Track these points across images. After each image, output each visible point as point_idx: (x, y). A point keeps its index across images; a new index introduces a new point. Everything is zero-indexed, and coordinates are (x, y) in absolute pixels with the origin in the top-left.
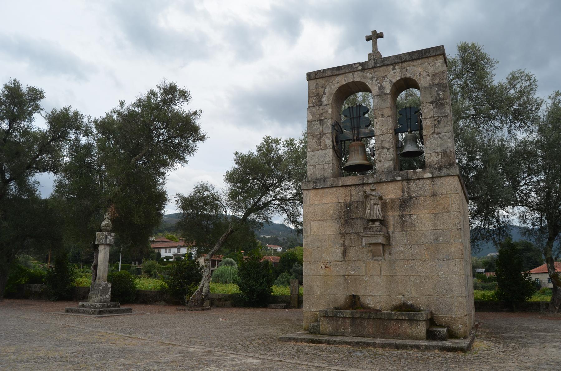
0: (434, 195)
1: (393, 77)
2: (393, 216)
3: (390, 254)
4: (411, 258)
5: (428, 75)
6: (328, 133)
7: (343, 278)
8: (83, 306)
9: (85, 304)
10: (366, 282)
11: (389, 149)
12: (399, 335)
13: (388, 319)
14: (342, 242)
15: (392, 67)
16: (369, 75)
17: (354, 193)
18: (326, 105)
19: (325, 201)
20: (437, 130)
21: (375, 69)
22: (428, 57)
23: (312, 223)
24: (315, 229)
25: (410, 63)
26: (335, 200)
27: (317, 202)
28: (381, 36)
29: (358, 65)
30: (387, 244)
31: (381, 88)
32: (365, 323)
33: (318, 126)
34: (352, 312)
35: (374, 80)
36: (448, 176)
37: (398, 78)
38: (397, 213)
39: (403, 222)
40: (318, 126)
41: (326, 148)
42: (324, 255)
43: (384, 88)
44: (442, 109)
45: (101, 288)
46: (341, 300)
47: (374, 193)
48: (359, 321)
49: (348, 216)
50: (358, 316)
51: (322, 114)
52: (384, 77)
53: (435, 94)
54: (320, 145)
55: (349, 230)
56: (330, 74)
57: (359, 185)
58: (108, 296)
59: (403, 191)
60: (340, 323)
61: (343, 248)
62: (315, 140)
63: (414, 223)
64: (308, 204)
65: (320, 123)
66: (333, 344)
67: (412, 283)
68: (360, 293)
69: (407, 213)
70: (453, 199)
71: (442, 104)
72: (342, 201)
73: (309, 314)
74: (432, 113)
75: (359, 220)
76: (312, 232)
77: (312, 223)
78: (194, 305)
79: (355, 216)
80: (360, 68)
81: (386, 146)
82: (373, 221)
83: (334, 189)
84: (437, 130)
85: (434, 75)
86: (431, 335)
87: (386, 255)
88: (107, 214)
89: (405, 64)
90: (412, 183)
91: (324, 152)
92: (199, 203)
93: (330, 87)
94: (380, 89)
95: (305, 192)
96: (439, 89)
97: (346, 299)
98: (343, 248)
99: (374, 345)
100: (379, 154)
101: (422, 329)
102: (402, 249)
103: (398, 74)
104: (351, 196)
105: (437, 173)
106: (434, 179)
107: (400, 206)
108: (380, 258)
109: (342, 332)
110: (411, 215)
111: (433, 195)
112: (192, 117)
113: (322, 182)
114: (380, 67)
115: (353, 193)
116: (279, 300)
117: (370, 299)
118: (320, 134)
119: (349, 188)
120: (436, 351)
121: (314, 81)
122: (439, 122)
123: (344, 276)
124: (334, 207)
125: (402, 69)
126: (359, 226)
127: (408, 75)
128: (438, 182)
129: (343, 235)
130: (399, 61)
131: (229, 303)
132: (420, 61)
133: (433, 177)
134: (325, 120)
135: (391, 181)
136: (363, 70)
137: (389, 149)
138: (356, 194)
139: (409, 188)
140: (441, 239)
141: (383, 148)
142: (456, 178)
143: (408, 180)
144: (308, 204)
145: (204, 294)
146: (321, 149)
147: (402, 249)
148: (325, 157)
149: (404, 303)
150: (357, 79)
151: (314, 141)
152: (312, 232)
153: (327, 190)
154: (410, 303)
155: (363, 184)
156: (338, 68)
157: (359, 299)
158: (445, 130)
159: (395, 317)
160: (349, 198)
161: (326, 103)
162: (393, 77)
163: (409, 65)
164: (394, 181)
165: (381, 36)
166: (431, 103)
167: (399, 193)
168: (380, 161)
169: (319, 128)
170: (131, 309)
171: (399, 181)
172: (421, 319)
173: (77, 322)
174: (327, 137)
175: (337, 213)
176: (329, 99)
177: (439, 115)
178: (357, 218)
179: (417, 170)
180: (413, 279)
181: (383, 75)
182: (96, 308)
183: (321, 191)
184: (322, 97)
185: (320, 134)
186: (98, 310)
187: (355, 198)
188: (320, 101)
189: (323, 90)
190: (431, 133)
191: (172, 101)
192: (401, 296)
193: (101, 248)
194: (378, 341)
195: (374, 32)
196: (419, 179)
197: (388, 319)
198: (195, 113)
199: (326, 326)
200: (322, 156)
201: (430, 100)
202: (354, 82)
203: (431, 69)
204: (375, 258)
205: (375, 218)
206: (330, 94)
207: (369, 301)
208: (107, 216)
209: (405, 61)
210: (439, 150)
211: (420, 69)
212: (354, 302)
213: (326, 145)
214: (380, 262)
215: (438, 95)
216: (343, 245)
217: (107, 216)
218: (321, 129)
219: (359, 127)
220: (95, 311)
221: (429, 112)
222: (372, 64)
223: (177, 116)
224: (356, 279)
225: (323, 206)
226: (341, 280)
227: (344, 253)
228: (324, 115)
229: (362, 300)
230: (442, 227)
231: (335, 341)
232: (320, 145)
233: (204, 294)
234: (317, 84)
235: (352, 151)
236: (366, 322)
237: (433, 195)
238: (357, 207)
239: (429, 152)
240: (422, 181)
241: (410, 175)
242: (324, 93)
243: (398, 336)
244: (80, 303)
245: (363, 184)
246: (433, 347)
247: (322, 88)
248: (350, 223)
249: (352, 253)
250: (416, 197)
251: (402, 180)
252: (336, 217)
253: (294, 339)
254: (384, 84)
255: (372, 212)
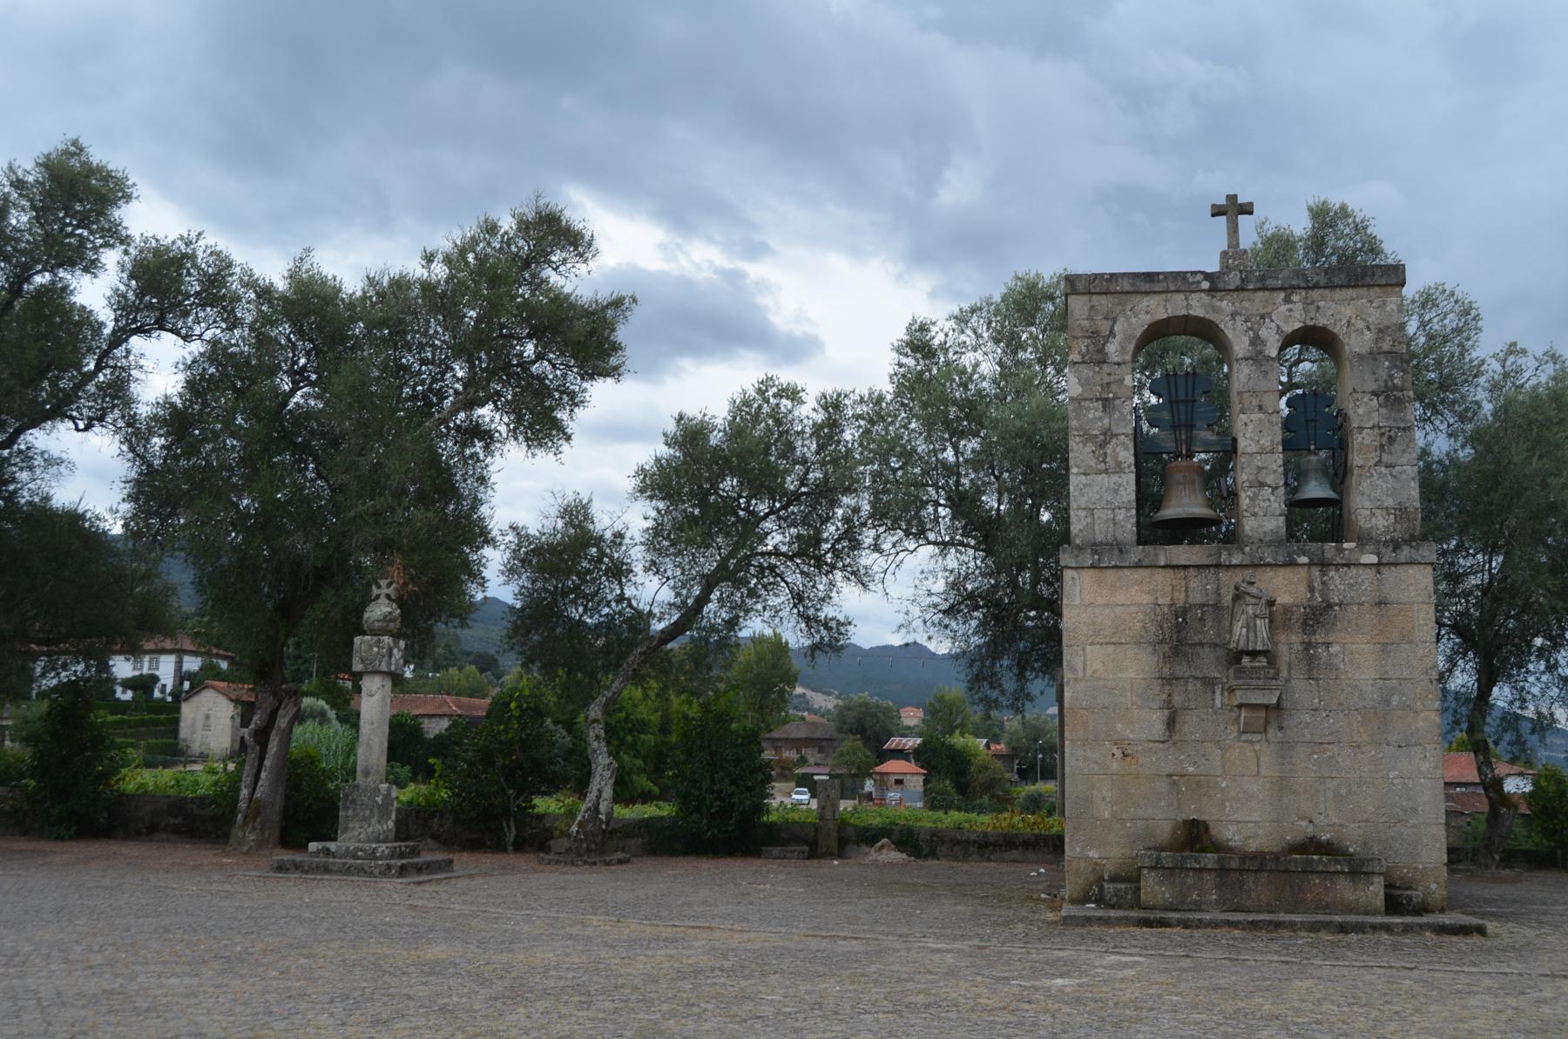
0: (1381, 603)
1: (1287, 319)
2: (1289, 644)
3: (1281, 728)
4: (1329, 739)
5: (1368, 328)
6: (1127, 435)
7: (1167, 780)
8: (327, 852)
9: (332, 846)
10: (1222, 790)
11: (1275, 489)
12: (1327, 907)
13: (1304, 872)
14: (1164, 697)
15: (1282, 295)
16: (1226, 305)
17: (1194, 584)
18: (1118, 364)
19: (1121, 598)
20: (1386, 458)
21: (1245, 294)
22: (1368, 286)
23: (1089, 648)
24: (1097, 665)
25: (1327, 292)
26: (1147, 599)
27: (1100, 601)
28: (1247, 209)
29: (1199, 277)
30: (1275, 712)
31: (1256, 341)
32: (1250, 881)
33: (1099, 414)
34: (1220, 859)
35: (1239, 319)
36: (1412, 563)
37: (1298, 325)
38: (1296, 639)
39: (1310, 659)
40: (1099, 414)
41: (1119, 469)
42: (1119, 726)
43: (1263, 343)
44: (1400, 411)
45: (379, 799)
46: (1164, 830)
47: (1253, 590)
48: (1235, 876)
49: (1178, 637)
50: (1234, 865)
51: (1108, 384)
52: (1263, 317)
53: (1383, 374)
54: (1104, 461)
55: (1181, 670)
56: (1127, 287)
57: (1208, 566)
58: (391, 824)
59: (1311, 589)
60: (1190, 881)
61: (1166, 712)
62: (1090, 447)
63: (1335, 661)
64: (1077, 601)
65: (1104, 407)
66: (1197, 927)
67: (1330, 794)
68: (1209, 814)
69: (1319, 638)
70: (1423, 614)
71: (1397, 399)
72: (1164, 601)
73: (1083, 865)
74: (1375, 418)
75: (1207, 649)
76: (1089, 672)
77: (1089, 648)
78: (589, 851)
79: (1196, 640)
80: (1206, 285)
81: (1270, 480)
82: (1254, 654)
83: (1145, 572)
84: (1386, 458)
85: (1380, 330)
86: (1394, 904)
87: (1271, 730)
88: (383, 583)
89: (1315, 294)
90: (1332, 573)
91: (1115, 478)
92: (570, 556)
93: (1128, 319)
94: (1252, 343)
95: (1068, 574)
96: (1393, 366)
97: (1174, 829)
98: (1166, 712)
99: (1292, 926)
100: (1252, 499)
101: (1375, 892)
102: (1307, 718)
103: (1297, 314)
104: (1187, 591)
105: (1389, 556)
106: (1382, 569)
107: (1305, 624)
108: (1257, 737)
109: (1194, 902)
110: (1328, 645)
111: (1379, 604)
112: (610, 312)
113: (1116, 552)
114: (1255, 290)
115: (1192, 585)
116: (783, 835)
117: (1233, 828)
118: (1104, 434)
119: (1182, 573)
120: (1428, 934)
121: (1086, 298)
122: (1391, 440)
123: (1170, 776)
124: (1145, 614)
125: (1307, 304)
126: (1209, 664)
127: (1322, 321)
128: (1390, 574)
129: (1169, 680)
130: (1303, 284)
131: (636, 842)
132: (1350, 293)
133: (1379, 564)
134: (1117, 402)
135: (1285, 565)
136: (1213, 290)
137: (1275, 489)
138: (1199, 589)
139: (1324, 583)
140: (1395, 700)
141: (1262, 485)
142: (1429, 568)
143: (1324, 565)
144: (1077, 601)
145: (603, 817)
146: (1106, 471)
147: (1307, 718)
148: (1116, 491)
149: (1312, 839)
150: (1197, 311)
151: (1088, 449)
152: (1089, 672)
153: (1127, 572)
154: (1325, 837)
155: (1218, 566)
156: (1150, 277)
157: (1207, 828)
158: (1404, 460)
159: (1320, 868)
160: (1183, 596)
161: (1117, 359)
162: (1287, 319)
163: (1323, 298)
164: (1292, 564)
165: (1247, 209)
166: (1374, 393)
167: (1302, 594)
168: (1255, 515)
169: (1100, 419)
170: (451, 861)
171: (1303, 565)
172: (1377, 870)
173: (330, 893)
174: (1123, 444)
175: (1152, 628)
176: (1123, 350)
177: (1393, 424)
178: (1202, 644)
179: (1346, 545)
180: (1331, 784)
181: (1262, 311)
182: (377, 859)
183: (1110, 574)
184: (1106, 342)
185: (1104, 434)
186: (399, 862)
187: (1197, 597)
188: (1101, 351)
189: (1108, 324)
190: (1372, 462)
191: (540, 256)
192: (1304, 823)
193: (371, 684)
194: (1297, 918)
195: (1232, 198)
196: (1348, 565)
197: (1304, 872)
198: (617, 303)
199: (1154, 889)
200: (1108, 489)
201: (1372, 387)
202: (1187, 318)
203: (1374, 316)
204: (1244, 737)
205: (1259, 647)
206: (1127, 338)
207: (1231, 834)
208: (384, 591)
209: (1316, 286)
210: (1390, 502)
211: (1348, 312)
212: (1195, 836)
213: (1119, 464)
214: (1257, 747)
215: (1391, 377)
216: (1168, 704)
217: (384, 589)
218: (1106, 421)
219: (1190, 426)
220: (389, 867)
221: (1369, 413)
222: (1234, 279)
223: (561, 305)
224: (1199, 784)
225: (1118, 610)
226: (1162, 786)
227: (1171, 724)
228: (1114, 387)
229: (1213, 831)
230: (1398, 675)
231: (1200, 920)
232: (1104, 461)
233: (603, 817)
234: (1092, 307)
235: (1179, 483)
236: (1251, 880)
237: (1379, 604)
238: (1202, 619)
239: (1368, 505)
240: (1354, 570)
241: (1328, 555)
242: (1112, 333)
243: (1327, 908)
244: (313, 846)
245: (1218, 566)
246: (1420, 925)
247: (1106, 318)
248: (1185, 654)
249: (1189, 725)
250: (1341, 604)
251: (1310, 565)
252: (1152, 638)
253: (1100, 919)
254: (1263, 333)
255: (1251, 635)
